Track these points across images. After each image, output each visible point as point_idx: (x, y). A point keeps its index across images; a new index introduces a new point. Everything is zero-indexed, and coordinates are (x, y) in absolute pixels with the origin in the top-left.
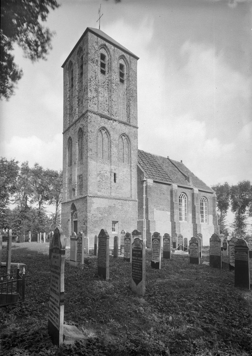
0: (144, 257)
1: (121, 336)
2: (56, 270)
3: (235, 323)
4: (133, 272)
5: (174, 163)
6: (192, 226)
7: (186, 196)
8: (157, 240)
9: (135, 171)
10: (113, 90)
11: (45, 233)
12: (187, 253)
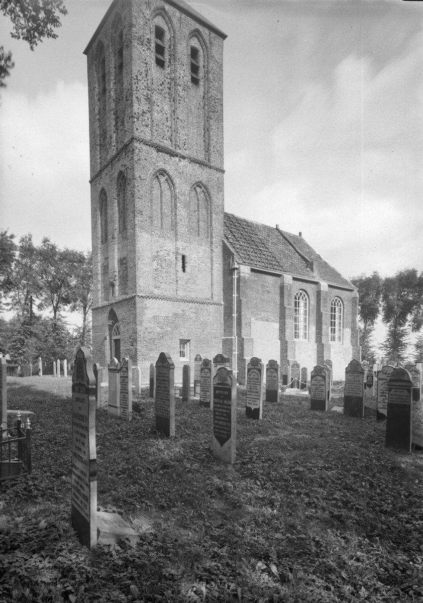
1: (195, 530)
2: (82, 422)
5: (288, 238)
6: (315, 347)
7: (306, 296)
8: (255, 370)
9: (218, 251)
10: (178, 98)
11: (66, 361)
12: (307, 393)
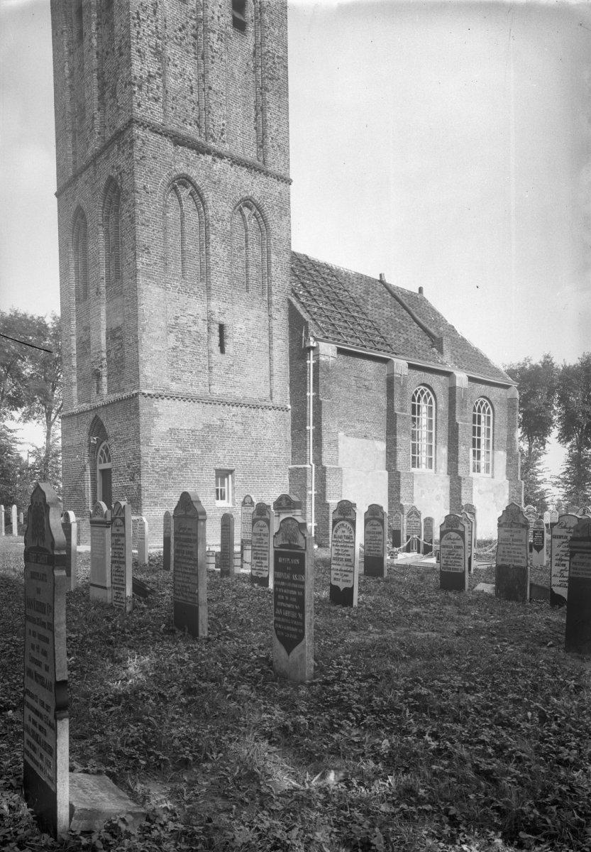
0: (309, 572)
1: (242, 801)
2: (42, 616)
3: (565, 753)
4: (276, 615)
5: (400, 296)
6: (447, 482)
7: (432, 396)
8: (346, 523)
9: (281, 318)
10: (211, 53)
11: (15, 507)
12: (433, 560)
